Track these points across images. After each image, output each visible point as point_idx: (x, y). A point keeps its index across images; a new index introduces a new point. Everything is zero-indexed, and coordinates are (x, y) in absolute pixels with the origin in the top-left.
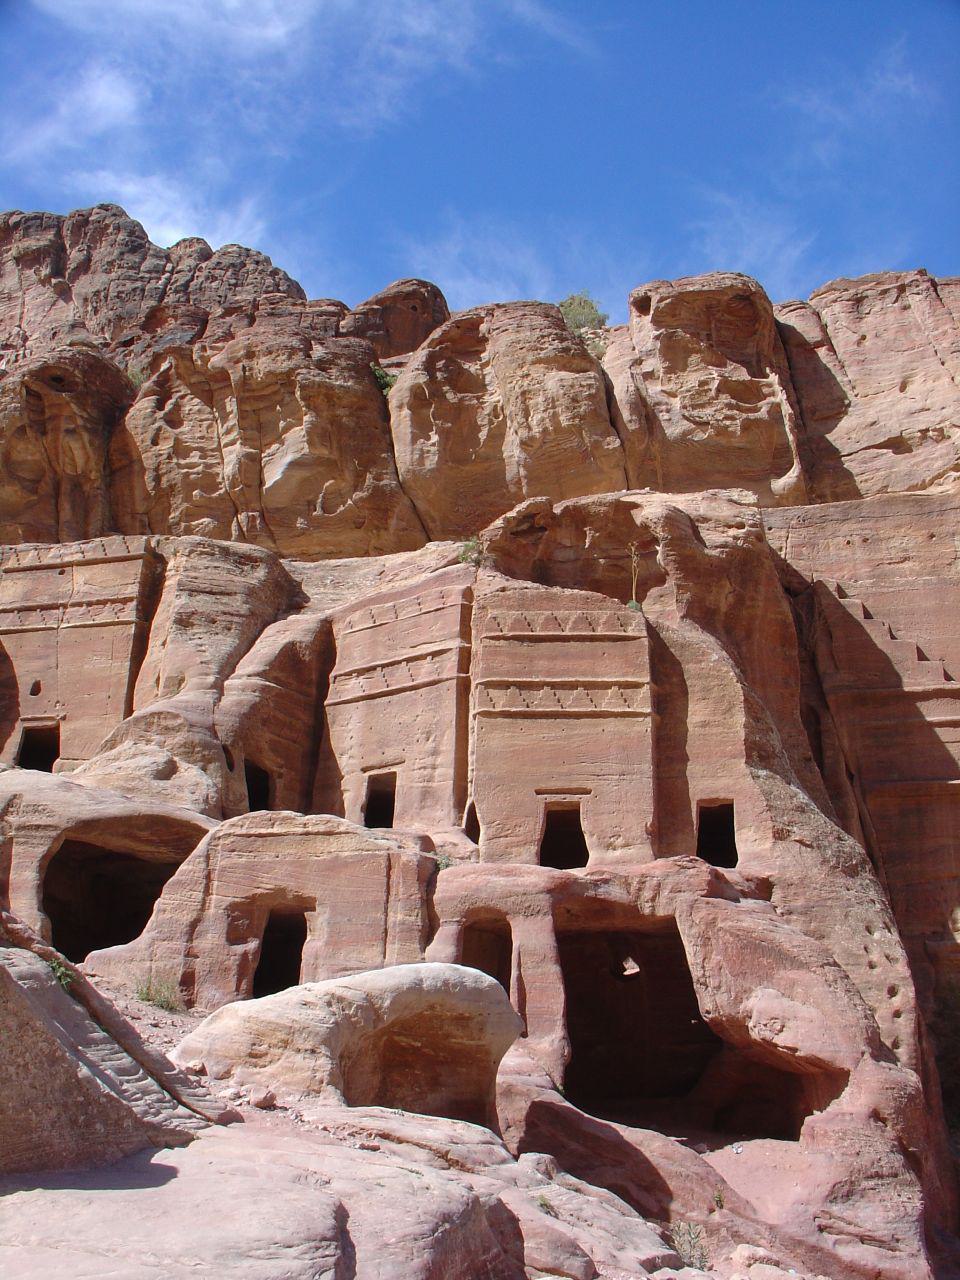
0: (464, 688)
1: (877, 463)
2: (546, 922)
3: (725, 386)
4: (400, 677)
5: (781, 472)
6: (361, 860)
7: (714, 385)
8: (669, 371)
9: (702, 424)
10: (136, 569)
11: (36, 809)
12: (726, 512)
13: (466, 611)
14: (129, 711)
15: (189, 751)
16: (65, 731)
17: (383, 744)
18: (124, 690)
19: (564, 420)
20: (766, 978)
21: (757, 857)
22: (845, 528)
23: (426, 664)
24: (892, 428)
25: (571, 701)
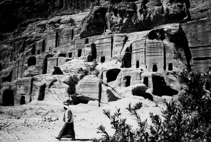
0: (145, 52)
1: (198, 14)
2: (151, 78)
3: (178, 6)
4: (139, 51)
5: (185, 17)
6: (135, 73)
7: (177, 6)
8: (171, 4)
9: (175, 12)
10: (111, 39)
11: (105, 69)
12: (174, 28)
13: (145, 43)
14: (112, 56)
15: (119, 61)
16: (105, 57)
17: (138, 58)
18: (111, 52)
19: (158, 13)
20: (172, 82)
21: (175, 69)
22: (192, 25)
23: (142, 49)
24: (201, 9)
25: (155, 54)
